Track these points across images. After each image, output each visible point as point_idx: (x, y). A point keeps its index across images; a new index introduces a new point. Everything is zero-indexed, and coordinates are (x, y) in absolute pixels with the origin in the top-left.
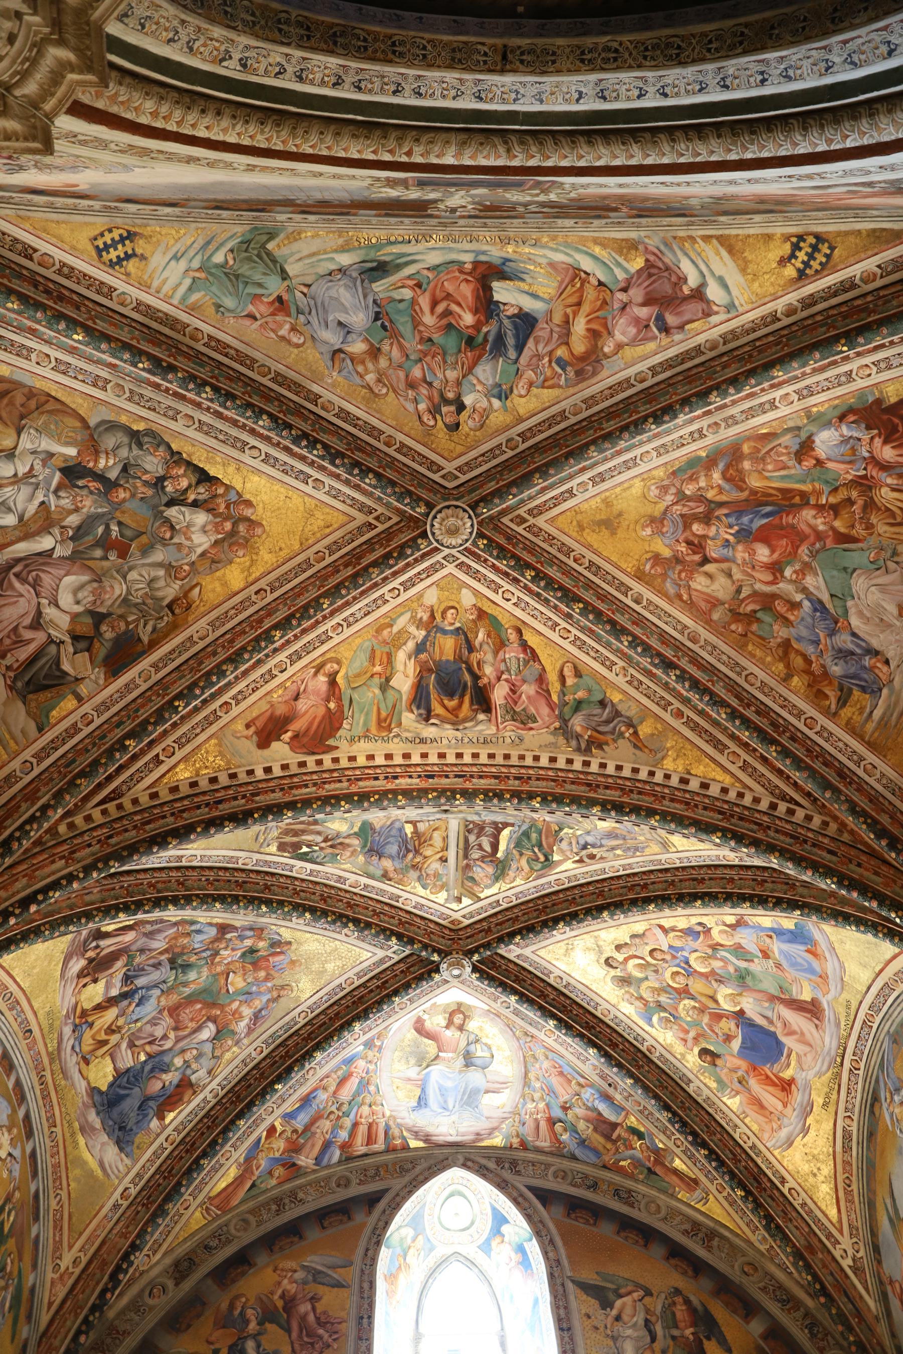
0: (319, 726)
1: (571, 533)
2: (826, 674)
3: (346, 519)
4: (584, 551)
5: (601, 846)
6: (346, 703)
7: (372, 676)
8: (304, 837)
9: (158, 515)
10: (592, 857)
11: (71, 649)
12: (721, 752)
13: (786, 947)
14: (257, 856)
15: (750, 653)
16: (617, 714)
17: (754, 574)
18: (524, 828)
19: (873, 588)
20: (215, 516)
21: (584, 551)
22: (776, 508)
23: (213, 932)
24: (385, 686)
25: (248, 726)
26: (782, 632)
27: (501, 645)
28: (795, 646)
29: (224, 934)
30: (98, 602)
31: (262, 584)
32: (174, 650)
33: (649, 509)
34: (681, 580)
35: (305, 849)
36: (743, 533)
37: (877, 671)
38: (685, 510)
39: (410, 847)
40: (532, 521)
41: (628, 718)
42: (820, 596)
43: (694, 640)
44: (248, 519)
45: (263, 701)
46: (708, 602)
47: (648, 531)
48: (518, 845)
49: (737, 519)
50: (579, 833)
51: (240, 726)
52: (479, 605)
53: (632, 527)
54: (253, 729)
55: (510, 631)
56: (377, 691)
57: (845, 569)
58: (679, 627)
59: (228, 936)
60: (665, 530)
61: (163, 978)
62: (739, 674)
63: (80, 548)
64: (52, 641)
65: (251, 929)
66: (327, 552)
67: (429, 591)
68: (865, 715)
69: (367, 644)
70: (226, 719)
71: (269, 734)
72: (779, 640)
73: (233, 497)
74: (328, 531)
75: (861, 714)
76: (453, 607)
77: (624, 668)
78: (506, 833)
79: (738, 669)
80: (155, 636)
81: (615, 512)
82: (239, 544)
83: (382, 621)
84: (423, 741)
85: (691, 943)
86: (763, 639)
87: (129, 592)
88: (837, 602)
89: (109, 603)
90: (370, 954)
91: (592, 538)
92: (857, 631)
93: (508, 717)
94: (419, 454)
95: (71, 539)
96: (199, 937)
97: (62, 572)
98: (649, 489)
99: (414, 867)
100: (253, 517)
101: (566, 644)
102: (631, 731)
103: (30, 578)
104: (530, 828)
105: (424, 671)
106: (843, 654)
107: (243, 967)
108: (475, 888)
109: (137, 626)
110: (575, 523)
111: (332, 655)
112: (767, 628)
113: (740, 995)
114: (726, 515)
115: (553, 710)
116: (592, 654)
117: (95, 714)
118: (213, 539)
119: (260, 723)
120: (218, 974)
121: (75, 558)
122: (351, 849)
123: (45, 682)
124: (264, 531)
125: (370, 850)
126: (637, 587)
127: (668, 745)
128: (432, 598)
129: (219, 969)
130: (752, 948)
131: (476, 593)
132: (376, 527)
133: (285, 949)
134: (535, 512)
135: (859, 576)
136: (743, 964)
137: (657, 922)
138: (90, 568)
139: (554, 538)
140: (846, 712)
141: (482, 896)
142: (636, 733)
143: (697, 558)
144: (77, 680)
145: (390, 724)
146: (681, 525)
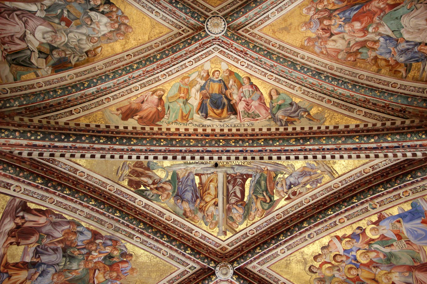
0: (153, 115)
1: (270, 35)
2: (397, 63)
3: (169, 30)
4: (276, 41)
5: (299, 184)
6: (166, 108)
7: (179, 98)
8: (142, 179)
9: (86, 13)
10: (294, 193)
11: (37, 56)
12: (353, 112)
13: (409, 225)
14: (116, 186)
15: (359, 67)
16: (299, 107)
17: (355, 35)
18: (257, 177)
19: (412, 19)
20: (111, 20)
21: (276, 41)
22: (360, 5)
23: (89, 236)
24: (186, 102)
25: (118, 110)
26: (372, 54)
27: (240, 85)
28: (380, 57)
29: (95, 239)
30: (54, 42)
31: (130, 52)
32: (86, 71)
33: (304, 19)
34: (322, 45)
35: (142, 188)
36: (347, 20)
37: (422, 51)
38: (320, 16)
39: (198, 195)
40: (252, 31)
41: (304, 108)
42: (387, 34)
43: (332, 69)
44: (125, 24)
45: (126, 101)
46: (335, 52)
47: (304, 28)
48: (255, 191)
49: (343, 14)
50: (286, 176)
51: (114, 109)
52: (230, 69)
53: (297, 28)
54: (120, 112)
55: (244, 79)
56: (182, 104)
57: (397, 18)
58: (324, 65)
59: (98, 241)
60: (311, 26)
61: (58, 261)
62: (355, 77)
63: (49, 16)
64: (29, 49)
65: (111, 240)
66: (160, 44)
67: (206, 63)
68: (421, 71)
69: (178, 85)
70: (107, 104)
71: (128, 115)
72: (372, 58)
73: (120, 13)
74: (161, 35)
75: (419, 71)
76: (217, 71)
77: (300, 88)
78: (248, 182)
79: (354, 75)
80: (78, 63)
81: (289, 23)
82: (121, 34)
83: (185, 75)
84: (203, 126)
85: (355, 244)
86: (364, 60)
87: (68, 41)
88: (396, 33)
89: (59, 43)
90: (177, 269)
91: (280, 36)
92: (408, 40)
93: (246, 116)
94: (201, 4)
95: (45, 10)
96: (81, 238)
97: (39, 23)
98: (302, 11)
99: (201, 209)
100: (128, 24)
101: (271, 82)
102: (307, 114)
103: (23, 19)
104: (260, 177)
105: (204, 98)
106: (404, 52)
107: (104, 267)
108: (234, 225)
109: (70, 57)
110: (271, 30)
111: (161, 87)
112: (365, 55)
113: (390, 272)
114: (338, 14)
115: (267, 110)
116: (284, 84)
117: (44, 84)
118: (109, 30)
119: (124, 110)
120: (89, 269)
121: (45, 19)
122: (167, 192)
123: (22, 63)
124: (132, 31)
125: (177, 195)
126: (302, 52)
127: (326, 116)
128: (208, 66)
129: (91, 265)
130: (390, 235)
131: (228, 63)
132: (182, 34)
133: (129, 259)
134: (253, 27)
135: (404, 18)
136: (387, 250)
137: (334, 234)
138: (52, 26)
139: (262, 37)
140: (411, 74)
141: (237, 230)
142: (309, 114)
143: (328, 35)
144: (38, 68)
145: (188, 118)
146: (318, 23)
